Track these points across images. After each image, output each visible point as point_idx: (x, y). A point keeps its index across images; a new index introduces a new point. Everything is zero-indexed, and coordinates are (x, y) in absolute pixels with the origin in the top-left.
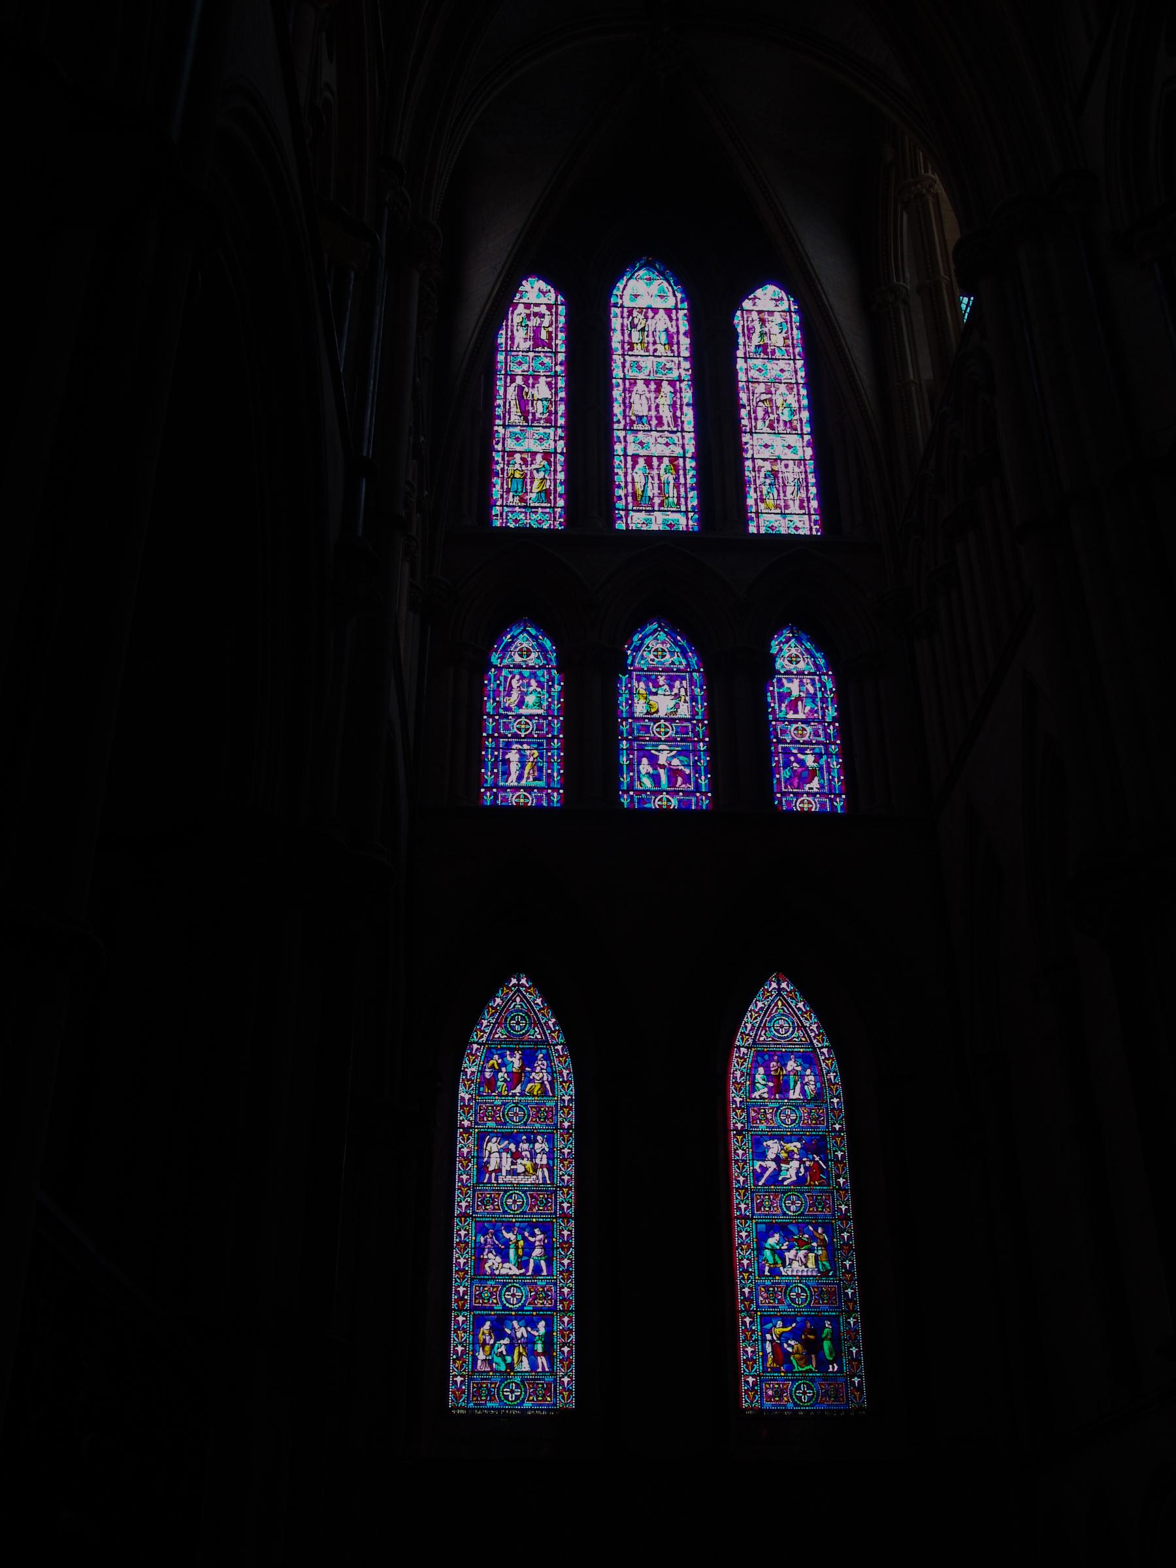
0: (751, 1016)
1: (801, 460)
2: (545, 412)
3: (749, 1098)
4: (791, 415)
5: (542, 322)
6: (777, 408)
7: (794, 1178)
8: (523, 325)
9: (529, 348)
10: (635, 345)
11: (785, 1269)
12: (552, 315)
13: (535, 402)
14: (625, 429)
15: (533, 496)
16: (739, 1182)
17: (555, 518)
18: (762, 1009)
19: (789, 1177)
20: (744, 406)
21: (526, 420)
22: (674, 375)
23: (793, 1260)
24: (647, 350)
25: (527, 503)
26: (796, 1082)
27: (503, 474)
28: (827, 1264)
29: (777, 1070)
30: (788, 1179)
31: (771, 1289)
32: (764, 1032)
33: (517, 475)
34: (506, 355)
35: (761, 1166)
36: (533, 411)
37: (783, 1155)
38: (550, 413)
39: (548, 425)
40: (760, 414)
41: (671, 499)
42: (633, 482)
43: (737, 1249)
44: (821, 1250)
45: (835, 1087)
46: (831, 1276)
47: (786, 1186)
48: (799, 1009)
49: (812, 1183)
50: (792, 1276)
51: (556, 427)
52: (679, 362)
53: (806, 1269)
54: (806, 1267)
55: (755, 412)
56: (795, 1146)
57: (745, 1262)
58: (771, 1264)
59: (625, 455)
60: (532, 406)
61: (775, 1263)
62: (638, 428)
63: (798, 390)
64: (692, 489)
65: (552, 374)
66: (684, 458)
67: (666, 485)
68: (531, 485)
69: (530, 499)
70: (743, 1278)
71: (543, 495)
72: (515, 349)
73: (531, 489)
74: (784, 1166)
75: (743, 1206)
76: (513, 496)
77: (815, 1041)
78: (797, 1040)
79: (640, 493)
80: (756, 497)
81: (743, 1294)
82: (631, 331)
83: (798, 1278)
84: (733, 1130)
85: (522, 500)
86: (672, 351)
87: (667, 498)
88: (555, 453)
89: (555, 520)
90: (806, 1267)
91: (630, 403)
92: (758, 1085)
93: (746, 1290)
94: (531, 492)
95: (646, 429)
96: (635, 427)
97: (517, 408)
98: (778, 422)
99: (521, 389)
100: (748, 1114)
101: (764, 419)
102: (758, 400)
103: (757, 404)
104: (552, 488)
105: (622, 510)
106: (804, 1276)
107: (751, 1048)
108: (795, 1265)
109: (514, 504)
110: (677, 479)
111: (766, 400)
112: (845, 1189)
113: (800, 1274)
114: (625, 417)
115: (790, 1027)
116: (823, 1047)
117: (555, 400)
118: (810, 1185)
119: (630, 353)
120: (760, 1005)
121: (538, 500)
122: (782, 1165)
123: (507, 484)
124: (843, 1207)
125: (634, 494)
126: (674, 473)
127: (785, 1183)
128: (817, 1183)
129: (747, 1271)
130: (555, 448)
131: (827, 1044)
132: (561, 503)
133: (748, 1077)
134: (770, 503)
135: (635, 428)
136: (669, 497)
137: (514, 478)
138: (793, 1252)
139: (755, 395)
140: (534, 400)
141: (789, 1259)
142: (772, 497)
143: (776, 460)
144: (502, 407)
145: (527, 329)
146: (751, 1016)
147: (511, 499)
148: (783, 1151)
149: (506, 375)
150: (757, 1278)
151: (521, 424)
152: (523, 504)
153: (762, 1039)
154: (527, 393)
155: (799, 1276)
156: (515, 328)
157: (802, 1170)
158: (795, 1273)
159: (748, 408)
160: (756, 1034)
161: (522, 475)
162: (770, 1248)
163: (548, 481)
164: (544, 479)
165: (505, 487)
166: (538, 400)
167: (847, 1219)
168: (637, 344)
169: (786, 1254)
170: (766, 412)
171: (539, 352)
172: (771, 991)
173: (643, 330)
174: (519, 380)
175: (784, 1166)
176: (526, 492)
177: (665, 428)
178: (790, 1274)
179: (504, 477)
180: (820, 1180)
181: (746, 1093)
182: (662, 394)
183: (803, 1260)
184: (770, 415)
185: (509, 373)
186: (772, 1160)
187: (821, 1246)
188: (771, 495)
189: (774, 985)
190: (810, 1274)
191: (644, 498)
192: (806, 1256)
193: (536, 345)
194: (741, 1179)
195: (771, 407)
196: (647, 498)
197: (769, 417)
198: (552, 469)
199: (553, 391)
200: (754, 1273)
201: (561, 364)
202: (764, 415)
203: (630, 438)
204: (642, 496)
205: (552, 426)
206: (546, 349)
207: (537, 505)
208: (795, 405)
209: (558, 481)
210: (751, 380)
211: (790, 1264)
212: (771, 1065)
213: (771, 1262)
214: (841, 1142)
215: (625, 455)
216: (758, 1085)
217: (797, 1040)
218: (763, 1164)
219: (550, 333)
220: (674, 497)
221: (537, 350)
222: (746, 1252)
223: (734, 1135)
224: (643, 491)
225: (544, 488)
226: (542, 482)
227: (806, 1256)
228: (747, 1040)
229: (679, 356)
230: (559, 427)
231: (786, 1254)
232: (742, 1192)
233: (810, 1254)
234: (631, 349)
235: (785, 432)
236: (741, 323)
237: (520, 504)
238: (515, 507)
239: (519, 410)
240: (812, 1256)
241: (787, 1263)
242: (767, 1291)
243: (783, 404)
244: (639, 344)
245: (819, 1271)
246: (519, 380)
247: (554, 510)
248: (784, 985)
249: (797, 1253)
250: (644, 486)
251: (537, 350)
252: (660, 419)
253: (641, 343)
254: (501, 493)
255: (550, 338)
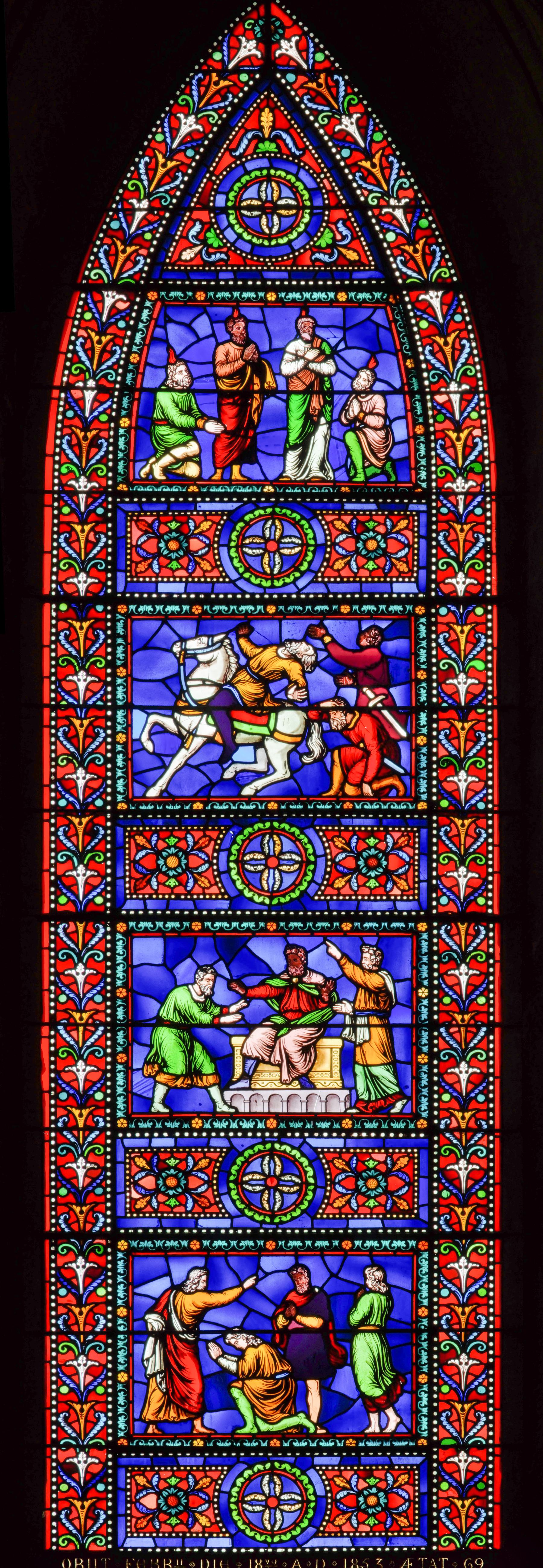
0: (151, 169)
3: (126, 481)
7: (282, 772)
11: (228, 1095)
16: (69, 787)
18: (192, 139)
19: (261, 766)
23: (258, 1061)
26: (310, 421)
28: (385, 1074)
29: (241, 372)
30: (260, 775)
31: (172, 1162)
32: (198, 227)
35: (158, 730)
37: (247, 689)
43: (53, 1023)
44: (369, 1026)
45: (463, 436)
46: (398, 1117)
47: (249, 799)
48: (344, 139)
49: (350, 790)
50: (251, 1116)
53: (304, 1094)
54: (306, 1082)
56: (294, 658)
57: (81, 1071)
58: (177, 1077)
61: (192, 1072)
70: (72, 1127)
74: (246, 731)
75: (81, 874)
77: (397, 263)
78: (326, 258)
81: (67, 1178)
83: (272, 1123)
84: (58, 600)
90: (306, 1082)
92: (162, 430)
93: (80, 1167)
100: (119, 540)
106: (297, 1117)
107: (143, 291)
108: (267, 1076)
112: (474, 812)
113: (280, 1108)
115: (300, 208)
116: (426, 286)
118: (341, 796)
120: (188, 125)
122: (237, 725)
124: (463, 877)
127: (248, 791)
128: (367, 789)
129: (84, 1100)
131: (446, 273)
133: (125, 401)
138: (261, 1036)
141: (246, 1058)
146: (151, 169)
148: (243, 676)
150: (122, 1123)
153: (187, 255)
155: (278, 1117)
157: (315, 744)
158: (261, 1108)
160: (166, 239)
162: (177, 1019)
167: (479, 918)
169: (237, 1041)
172: (238, 70)
175: (246, 731)
178: (243, 1108)
180: (378, 778)
181: (116, 461)
183: (296, 1058)
186: (203, 708)
187: (370, 1013)
189: (249, 48)
190: (317, 1108)
192: (308, 1049)
194: (81, 777)
200: (113, 1106)
211: (246, 1076)
212: (220, 357)
213: (177, 1064)
214: (473, 641)
216: (162, 430)
217: (326, 258)
218: (169, 723)
222: (87, 1035)
223: (61, 617)
227: (308, 1049)
228: (131, 260)
231: (237, 1041)
232: (80, 823)
233: (326, 1042)
240: (331, 1046)
241: (238, 1072)
242: (157, 1167)
245: (356, 1102)
248: (288, 48)
249: (276, 1038)
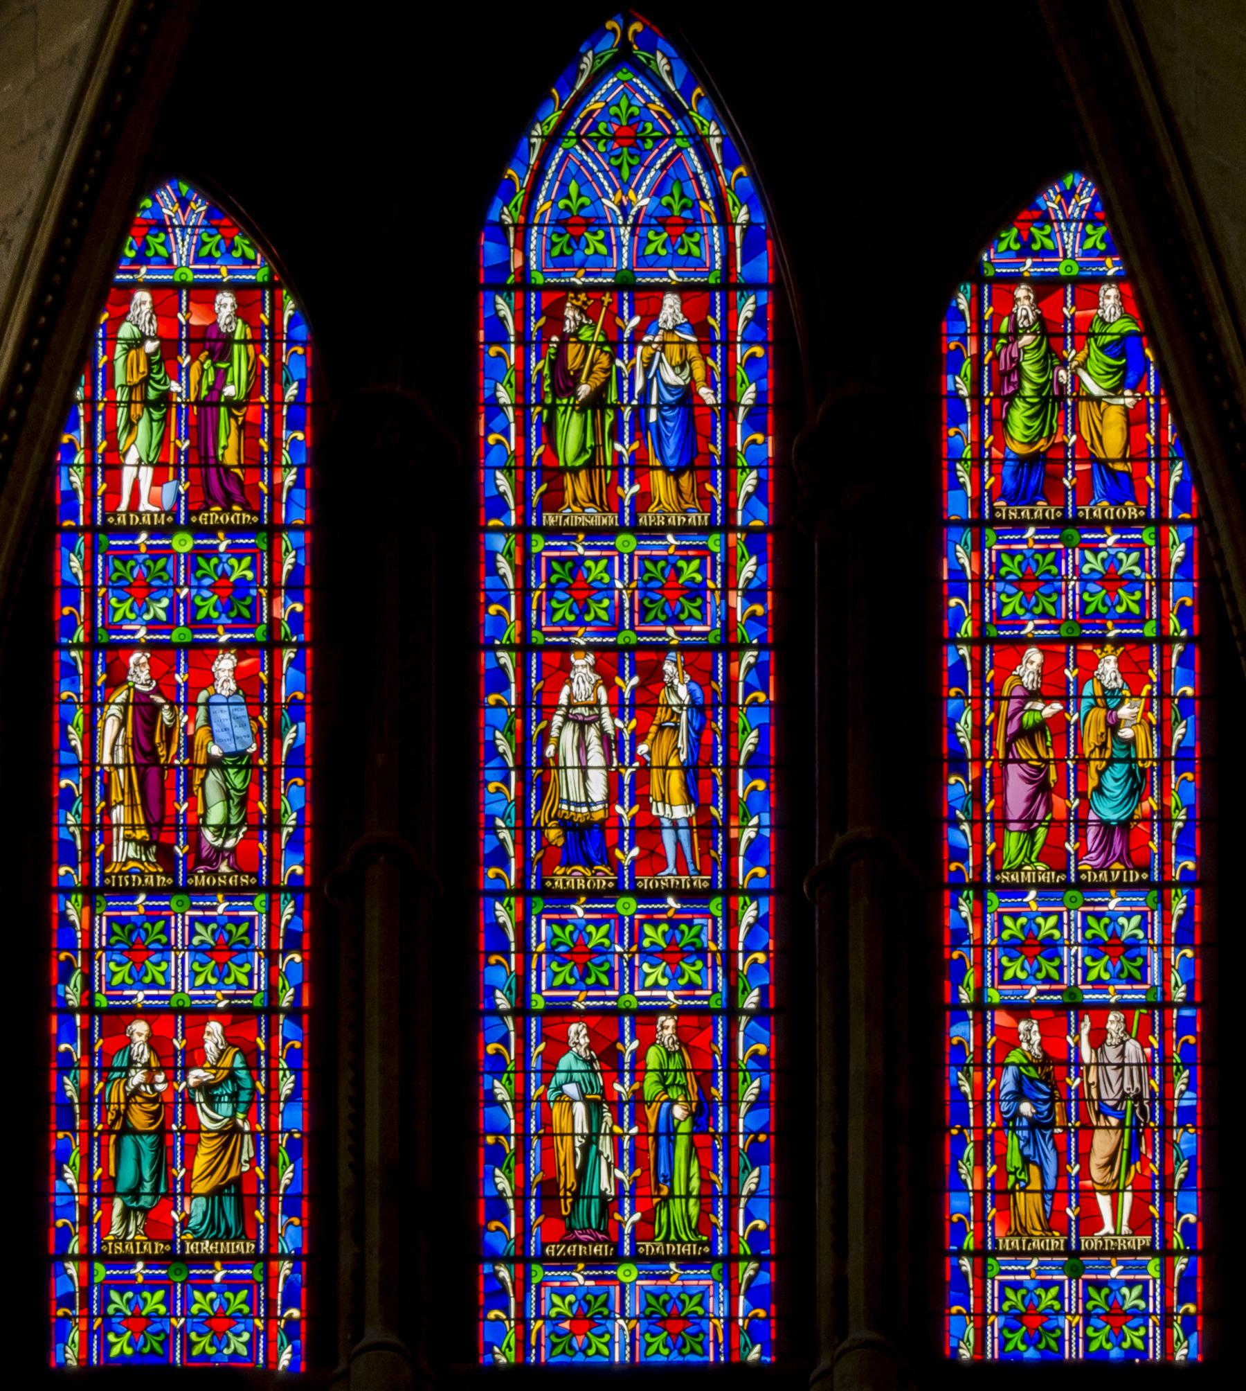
1: (1149, 1006)
2: (234, 821)
4: (1131, 794)
5: (221, 377)
6: (1082, 762)
8: (152, 395)
9: (174, 512)
10: (568, 479)
12: (257, 342)
13: (198, 775)
14: (523, 892)
15: (196, 1208)
17: (270, 1303)
20: (959, 763)
21: (166, 858)
22: (707, 629)
24: (615, 504)
25: (173, 1244)
27: (88, 1115)
33: (139, 1119)
34: (93, 549)
36: (191, 819)
38: (255, 829)
39: (245, 880)
40: (1018, 791)
41: (677, 1207)
42: (548, 1136)
51: (272, 890)
52: (728, 551)
55: (1000, 791)
59: (522, 1011)
60: (189, 795)
62: (570, 883)
63: (1164, 673)
64: (757, 1155)
65: (260, 634)
66: (731, 1011)
67: (663, 1139)
68: (188, 1164)
69: (185, 1223)
71: (229, 1204)
72: (121, 520)
73: (187, 1179)
76: (126, 1214)
79: (572, 1180)
80: (979, 1186)
82: (553, 408)
85: (157, 1227)
86: (706, 501)
87: (665, 1200)
88: (271, 1009)
89: (270, 1317)
91: (543, 762)
94: (187, 1193)
95: (601, 883)
96: (561, 878)
97: (133, 806)
98: (1081, 837)
99: (144, 710)
101: (1028, 824)
102: (1013, 727)
103: (1008, 747)
104: (260, 1171)
105: (507, 1260)
109: (129, 1248)
110: (702, 1114)
111: (1040, 727)
114: (524, 827)
117: (270, 764)
119: (550, 519)
121: (214, 1231)
123: (103, 1163)
125: (549, 1192)
126: (693, 1087)
130: (272, 992)
132: (290, 1236)
134: (1029, 1205)
135: (559, 884)
136: (671, 1195)
137: (127, 1130)
139: (1004, 704)
140: (194, 765)
142: (1036, 1185)
143: (1061, 1009)
144: (78, 805)
145: (165, 419)
147: (116, 1229)
149: (91, 646)
151: (149, 881)
152: (160, 1247)
154: (169, 732)
156: (121, 413)
159: (972, 774)
161: (155, 1115)
163: (247, 1138)
164: (230, 1133)
165: (98, 1172)
166: (212, 763)
168: (575, 471)
170: (1041, 789)
171: (210, 531)
173: (597, 402)
174: (139, 670)
176: (170, 1194)
177: (669, 876)
179: (91, 1129)
182: (661, 714)
184: (1056, 799)
185: (103, 637)
188: (1034, 1170)
191: (582, 1205)
193: (200, 498)
195: (1060, 762)
196: (595, 1204)
197: (1049, 808)
198: (260, 1086)
199: (263, 720)
201: (294, 590)
202: (1031, 799)
203: (543, 931)
204: (576, 1196)
205: (258, 888)
206: (239, 516)
207: (207, 1247)
208: (1146, 749)
209: (283, 1140)
210: (992, 632)
215: (522, 1011)
219: (248, 431)
220: (688, 1195)
221: (203, 518)
224: (581, 1175)
225: (233, 1173)
226: (225, 1146)
229: (728, 526)
230: (285, 890)
234: (553, 501)
235: (1103, 876)
236: (971, 348)
237: (147, 1248)
238: (128, 1261)
239: (140, 819)
243: (1103, 747)
244: (583, 475)
246: (139, 670)
247: (266, 1272)
250: (585, 1149)
251: (203, 518)
252: (646, 830)
253: (590, 466)
254: (84, 1199)
255: (253, 460)
